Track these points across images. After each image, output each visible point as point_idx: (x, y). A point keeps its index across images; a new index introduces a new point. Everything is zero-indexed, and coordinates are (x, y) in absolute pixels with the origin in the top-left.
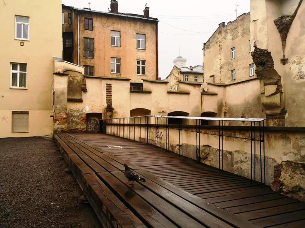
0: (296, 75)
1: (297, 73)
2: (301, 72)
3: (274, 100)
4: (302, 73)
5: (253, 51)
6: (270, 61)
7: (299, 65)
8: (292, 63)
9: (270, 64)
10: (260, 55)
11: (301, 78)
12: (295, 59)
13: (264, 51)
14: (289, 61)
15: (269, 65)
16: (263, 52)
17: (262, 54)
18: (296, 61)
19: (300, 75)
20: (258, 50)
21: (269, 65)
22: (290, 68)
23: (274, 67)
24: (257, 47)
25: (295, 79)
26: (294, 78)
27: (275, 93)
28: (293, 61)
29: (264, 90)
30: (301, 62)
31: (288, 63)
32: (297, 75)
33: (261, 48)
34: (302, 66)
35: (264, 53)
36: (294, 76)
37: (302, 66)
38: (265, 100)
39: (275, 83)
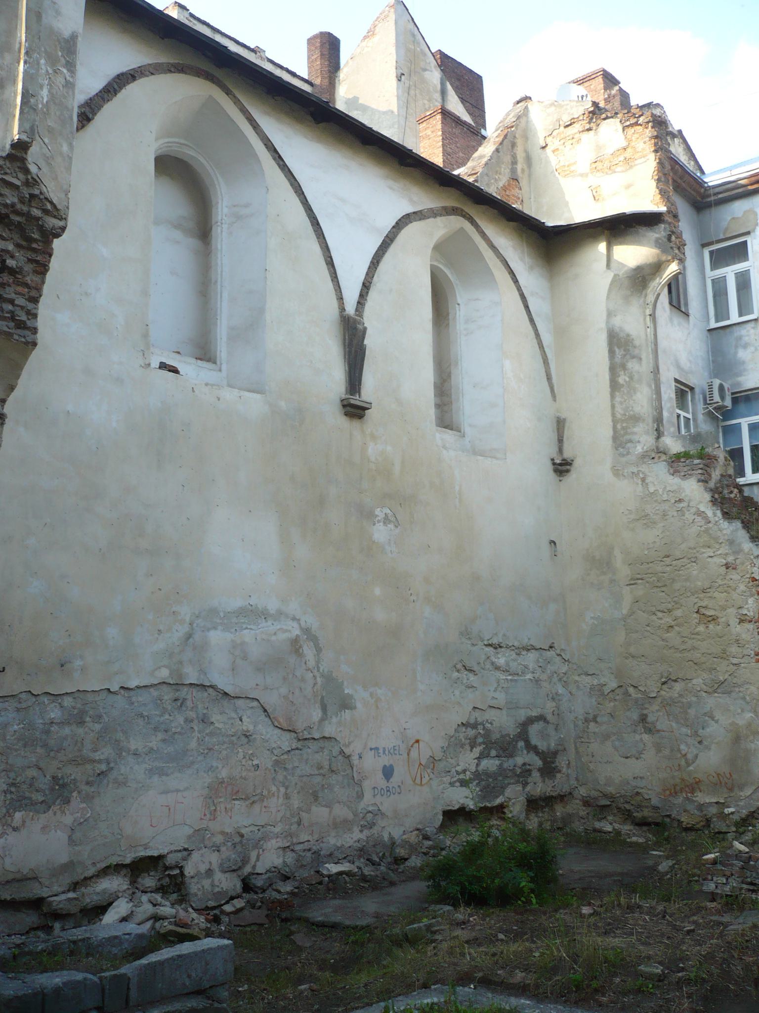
6: (26, 285)
9: (20, 301)
13: (46, 212)
15: (12, 302)
16: (36, 212)
17: (17, 219)
21: (12, 302)
23: (35, 330)
35: (38, 219)
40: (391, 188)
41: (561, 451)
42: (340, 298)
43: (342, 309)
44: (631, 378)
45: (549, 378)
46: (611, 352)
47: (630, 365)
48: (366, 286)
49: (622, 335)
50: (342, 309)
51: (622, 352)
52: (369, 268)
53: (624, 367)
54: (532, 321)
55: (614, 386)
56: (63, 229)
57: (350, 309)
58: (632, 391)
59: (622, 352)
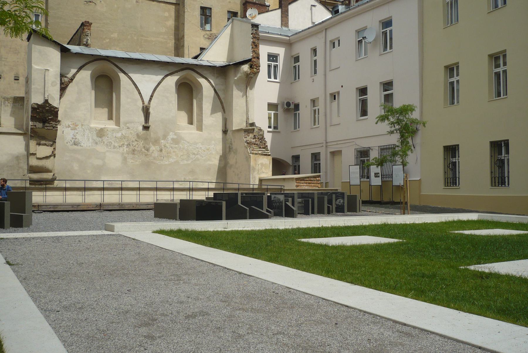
0: (70, 140)
1: (71, 139)
2: (76, 138)
3: (46, 163)
4: (77, 140)
5: (39, 103)
7: (73, 131)
8: (66, 126)
10: (47, 111)
11: (75, 144)
12: (69, 124)
14: (61, 123)
15: (52, 124)
18: (71, 126)
19: (74, 141)
20: (47, 105)
21: (52, 124)
22: (63, 132)
23: (57, 127)
24: (49, 101)
25: (68, 145)
26: (67, 143)
27: (50, 156)
28: (67, 125)
29: (36, 151)
30: (76, 128)
31: (60, 125)
32: (71, 141)
33: (53, 105)
34: (77, 133)
36: (67, 140)
37: (77, 133)
38: (34, 162)
39: (51, 146)
42: (143, 101)
43: (143, 103)
48: (152, 96)
50: (143, 103)
52: (153, 92)
56: (58, 110)
57: (146, 103)
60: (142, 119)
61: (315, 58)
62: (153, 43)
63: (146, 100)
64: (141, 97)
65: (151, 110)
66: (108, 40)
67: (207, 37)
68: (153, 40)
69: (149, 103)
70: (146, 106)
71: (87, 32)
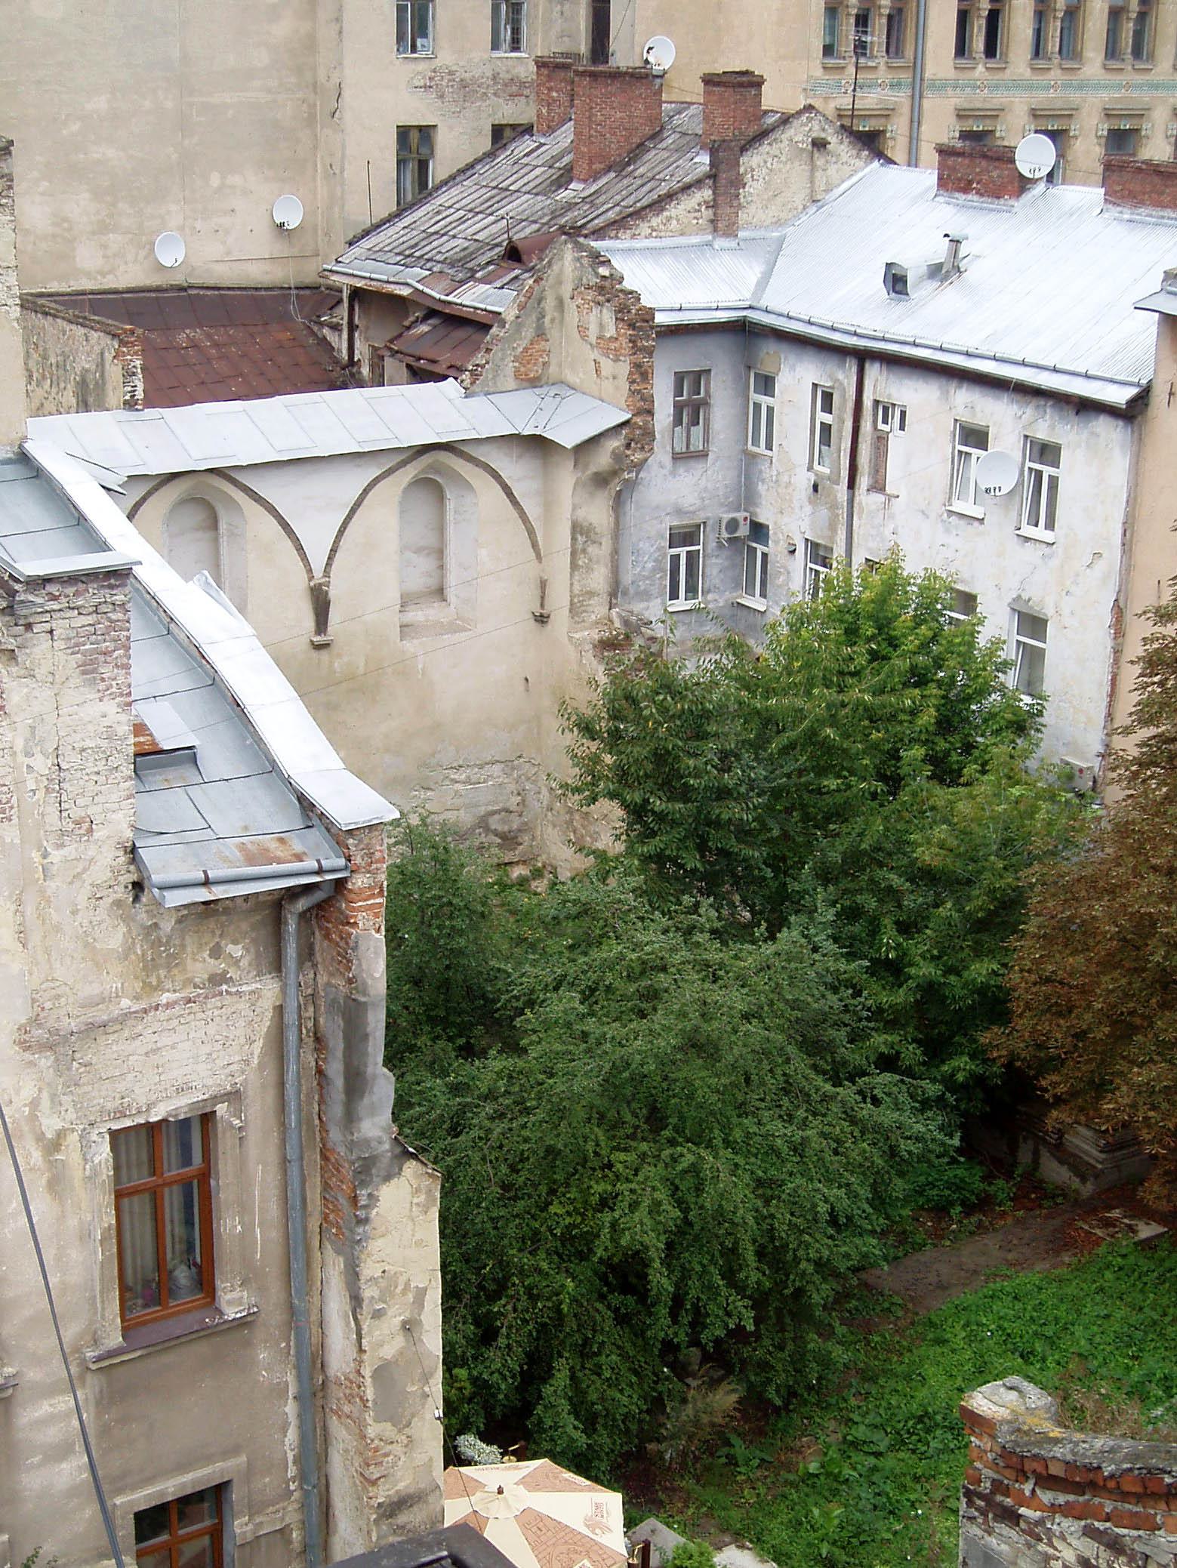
40: (359, 466)
41: (542, 606)
42: (310, 571)
43: (311, 578)
44: (590, 560)
45: (535, 545)
46: (574, 539)
47: (589, 550)
48: (334, 551)
49: (585, 524)
50: (311, 578)
51: (584, 539)
53: (584, 551)
54: (515, 502)
55: (574, 566)
58: (589, 569)
59: (584, 539)
60: (309, 622)
61: (827, 418)
62: (231, 112)
63: (318, 563)
64: (302, 560)
65: (333, 593)
66: (75, 127)
67: (422, 83)
68: (229, 101)
69: (327, 572)
70: (320, 585)
71: (132, 364)
